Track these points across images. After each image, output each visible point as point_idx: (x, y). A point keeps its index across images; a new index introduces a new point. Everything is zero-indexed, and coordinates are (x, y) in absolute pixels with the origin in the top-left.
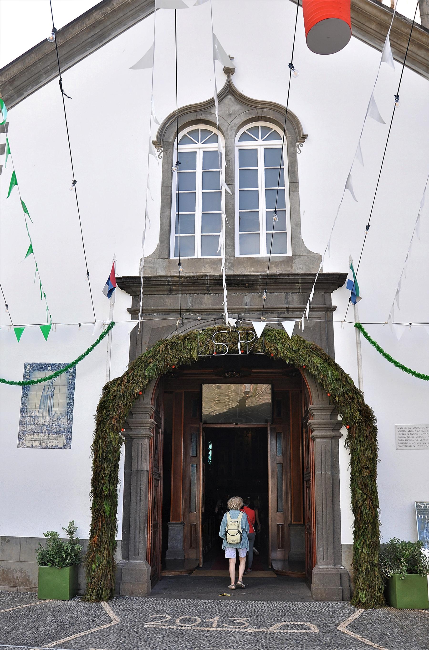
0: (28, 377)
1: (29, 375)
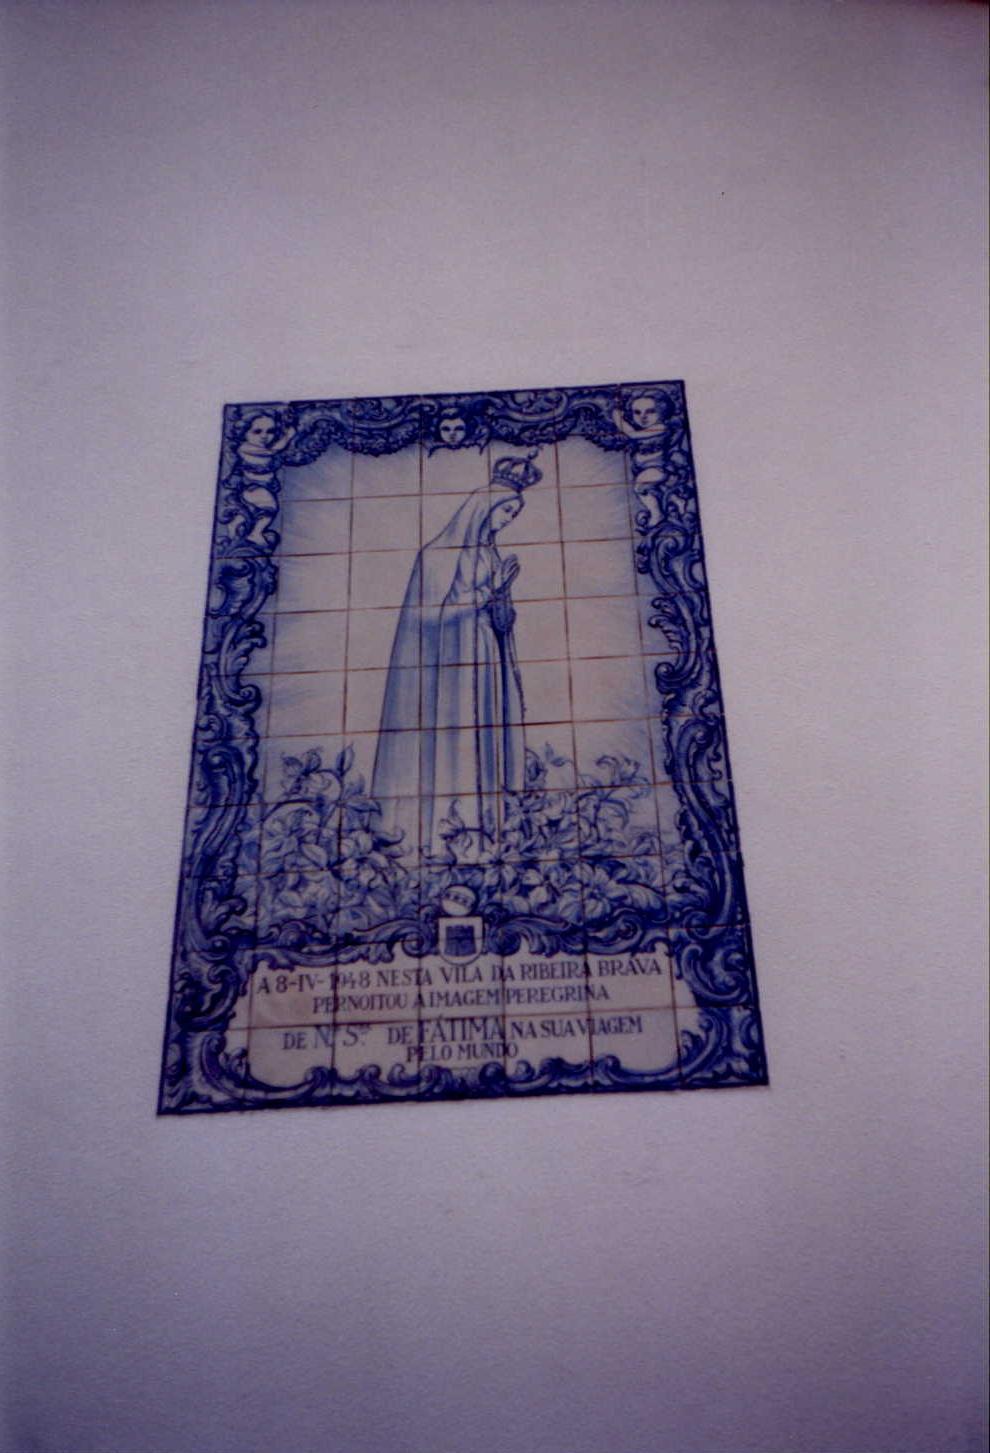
0: (260, 498)
1: (274, 488)
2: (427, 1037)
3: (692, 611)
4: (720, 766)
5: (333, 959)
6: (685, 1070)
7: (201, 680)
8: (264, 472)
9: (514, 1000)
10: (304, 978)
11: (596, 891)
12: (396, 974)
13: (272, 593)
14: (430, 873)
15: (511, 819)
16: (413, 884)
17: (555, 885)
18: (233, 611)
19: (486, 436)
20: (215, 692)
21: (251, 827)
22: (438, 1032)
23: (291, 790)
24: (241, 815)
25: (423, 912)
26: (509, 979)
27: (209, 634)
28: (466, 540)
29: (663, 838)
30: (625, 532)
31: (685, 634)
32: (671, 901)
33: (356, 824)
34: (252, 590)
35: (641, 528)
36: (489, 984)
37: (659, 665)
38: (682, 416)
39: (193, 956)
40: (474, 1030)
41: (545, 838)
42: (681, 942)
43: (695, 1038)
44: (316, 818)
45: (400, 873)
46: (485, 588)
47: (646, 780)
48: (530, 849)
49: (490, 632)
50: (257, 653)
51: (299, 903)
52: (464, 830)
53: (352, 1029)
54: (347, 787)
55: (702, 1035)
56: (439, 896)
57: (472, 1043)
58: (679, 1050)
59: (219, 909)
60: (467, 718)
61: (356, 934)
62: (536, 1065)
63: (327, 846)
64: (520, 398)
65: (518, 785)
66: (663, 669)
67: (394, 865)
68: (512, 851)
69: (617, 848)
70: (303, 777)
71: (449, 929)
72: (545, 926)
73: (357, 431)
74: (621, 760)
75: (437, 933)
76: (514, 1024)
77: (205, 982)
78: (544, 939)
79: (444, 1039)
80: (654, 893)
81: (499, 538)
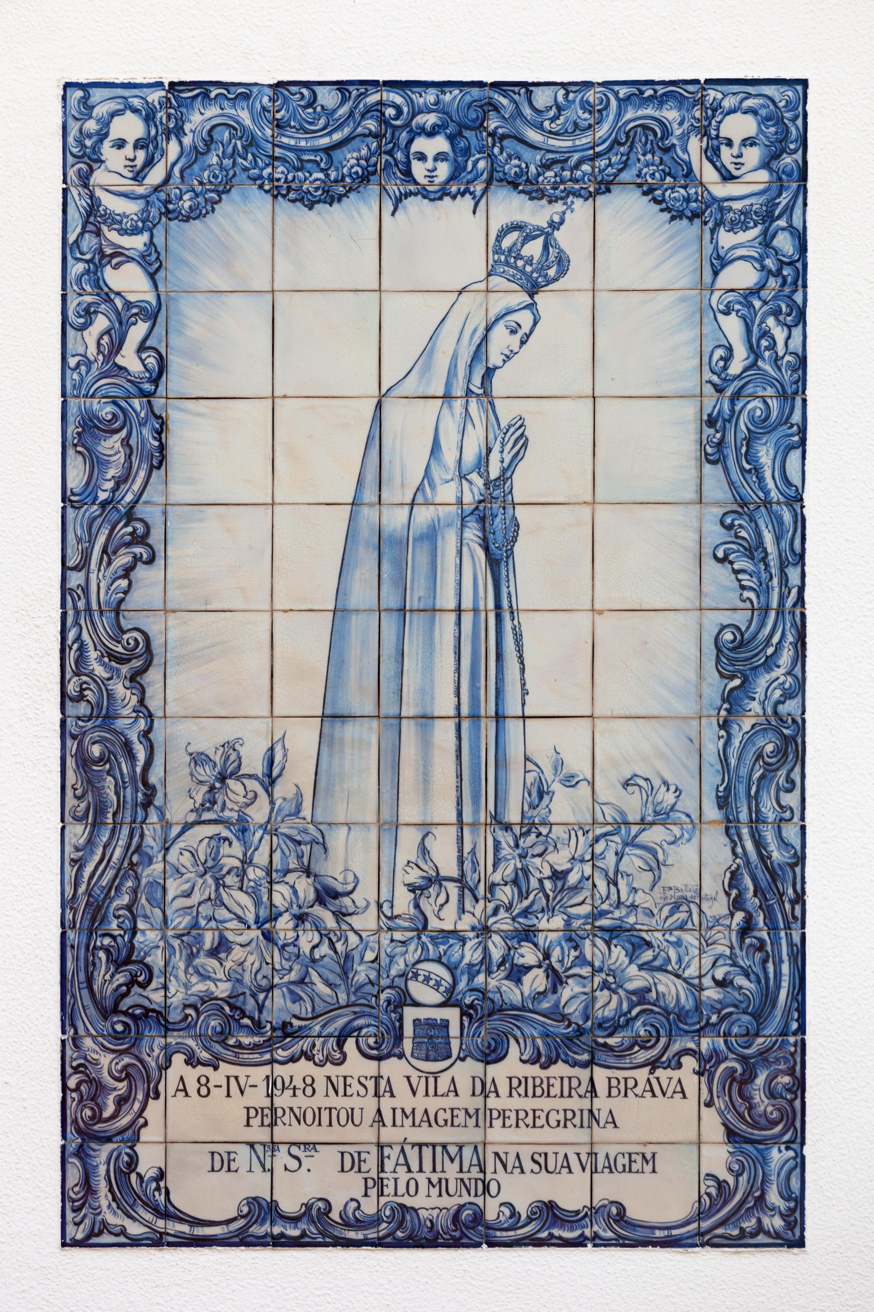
2: (389, 1165)
3: (778, 539)
4: (791, 799)
5: (267, 1056)
6: (705, 1225)
7: (64, 616)
8: (135, 231)
9: (497, 1123)
10: (232, 1080)
11: (611, 979)
12: (349, 1080)
13: (159, 468)
14: (392, 941)
15: (502, 865)
16: (370, 956)
17: (557, 966)
18: (103, 496)
19: (485, 176)
20: (85, 636)
21: (150, 861)
22: (402, 1160)
23: (202, 805)
24: (136, 839)
25: (383, 996)
26: (493, 1095)
27: (70, 536)
28: (448, 385)
29: (705, 907)
30: (691, 384)
31: (764, 575)
32: (708, 997)
33: (293, 864)
34: (129, 457)
35: (715, 379)
36: (466, 1100)
37: (723, 628)
38: (798, 156)
39: (88, 1042)
40: (447, 1160)
41: (547, 897)
42: (716, 1057)
43: (721, 1184)
44: (237, 849)
45: (353, 939)
46: (474, 477)
47: (688, 816)
48: (525, 913)
49: (481, 554)
50: (141, 571)
51: (220, 975)
52: (436, 880)
53: (295, 1150)
54: (278, 803)
55: (731, 1180)
56: (403, 975)
57: (442, 1175)
58: (700, 1197)
59: (117, 976)
60: (445, 704)
61: (296, 1023)
62: (523, 1209)
63: (254, 895)
64: (542, 98)
65: (513, 816)
66: (728, 636)
67: (344, 927)
68: (502, 914)
69: (642, 918)
70: (218, 785)
71: (416, 1022)
72: (542, 1024)
73: (278, 152)
74: (657, 783)
75: (401, 1027)
76: (497, 1154)
77: (107, 1080)
78: (539, 1042)
79: (409, 1170)
80: (685, 985)
81: (498, 384)
